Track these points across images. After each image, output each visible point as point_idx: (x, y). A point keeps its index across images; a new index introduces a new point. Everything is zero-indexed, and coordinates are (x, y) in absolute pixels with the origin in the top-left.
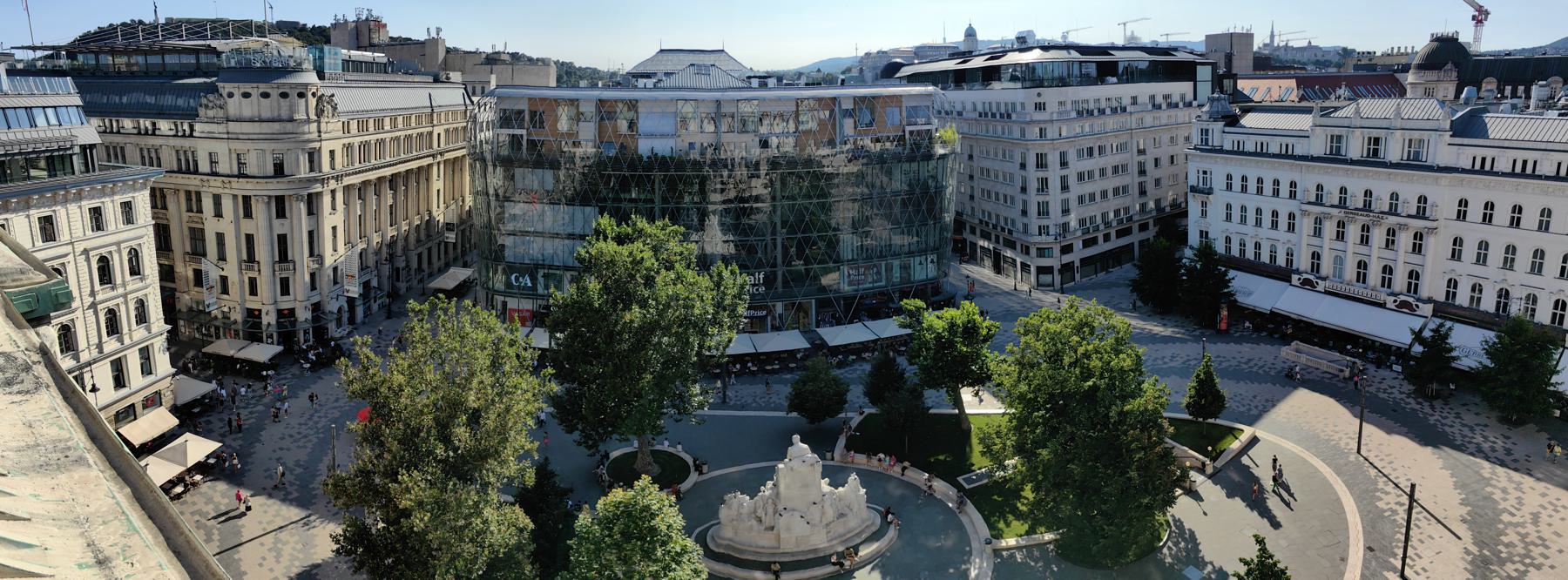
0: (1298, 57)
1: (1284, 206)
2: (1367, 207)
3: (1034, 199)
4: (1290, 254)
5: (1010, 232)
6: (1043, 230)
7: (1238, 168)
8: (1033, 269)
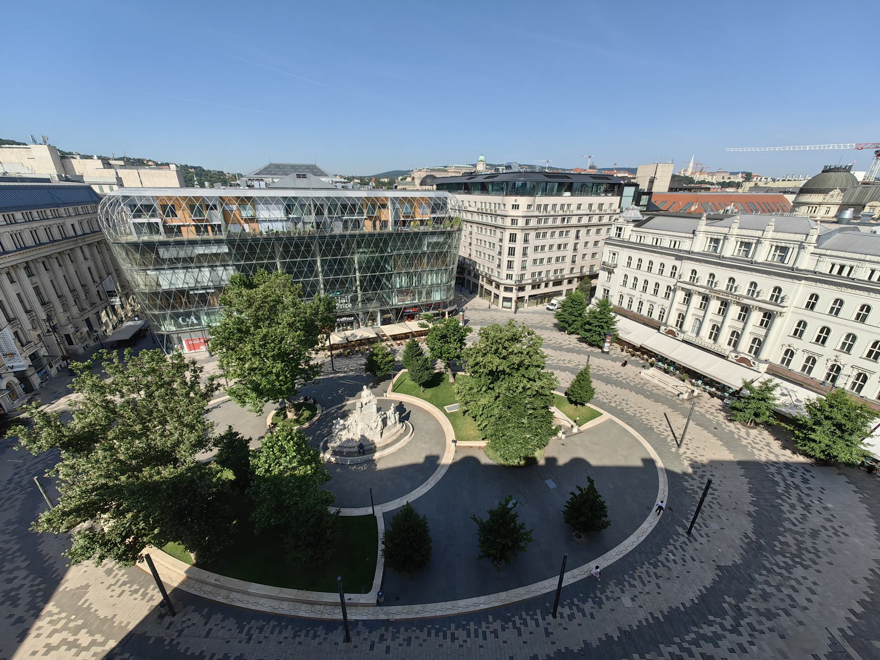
4: (662, 312)
6: (509, 276)
8: (501, 299)
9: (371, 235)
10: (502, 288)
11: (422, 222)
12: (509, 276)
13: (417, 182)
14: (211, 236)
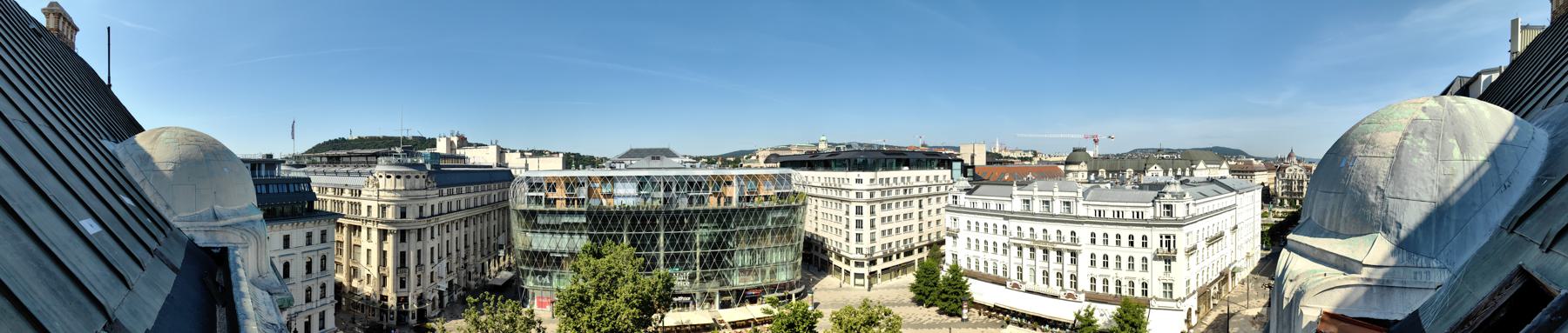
9: (715, 211)
11: (766, 197)
12: (859, 250)
13: (762, 160)
14: (576, 208)
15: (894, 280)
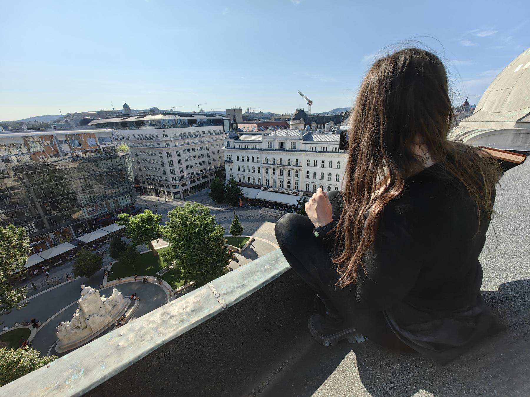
0: (257, 116)
1: (256, 165)
2: (281, 164)
3: (168, 169)
4: (259, 180)
5: (160, 181)
6: (174, 179)
7: (240, 153)
10: (171, 187)
15: (198, 192)
